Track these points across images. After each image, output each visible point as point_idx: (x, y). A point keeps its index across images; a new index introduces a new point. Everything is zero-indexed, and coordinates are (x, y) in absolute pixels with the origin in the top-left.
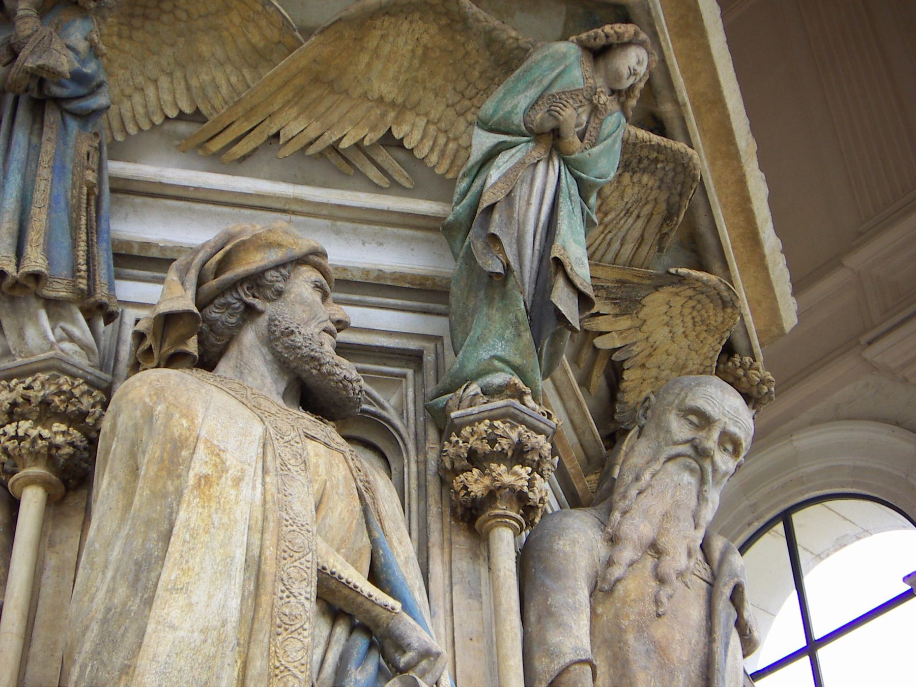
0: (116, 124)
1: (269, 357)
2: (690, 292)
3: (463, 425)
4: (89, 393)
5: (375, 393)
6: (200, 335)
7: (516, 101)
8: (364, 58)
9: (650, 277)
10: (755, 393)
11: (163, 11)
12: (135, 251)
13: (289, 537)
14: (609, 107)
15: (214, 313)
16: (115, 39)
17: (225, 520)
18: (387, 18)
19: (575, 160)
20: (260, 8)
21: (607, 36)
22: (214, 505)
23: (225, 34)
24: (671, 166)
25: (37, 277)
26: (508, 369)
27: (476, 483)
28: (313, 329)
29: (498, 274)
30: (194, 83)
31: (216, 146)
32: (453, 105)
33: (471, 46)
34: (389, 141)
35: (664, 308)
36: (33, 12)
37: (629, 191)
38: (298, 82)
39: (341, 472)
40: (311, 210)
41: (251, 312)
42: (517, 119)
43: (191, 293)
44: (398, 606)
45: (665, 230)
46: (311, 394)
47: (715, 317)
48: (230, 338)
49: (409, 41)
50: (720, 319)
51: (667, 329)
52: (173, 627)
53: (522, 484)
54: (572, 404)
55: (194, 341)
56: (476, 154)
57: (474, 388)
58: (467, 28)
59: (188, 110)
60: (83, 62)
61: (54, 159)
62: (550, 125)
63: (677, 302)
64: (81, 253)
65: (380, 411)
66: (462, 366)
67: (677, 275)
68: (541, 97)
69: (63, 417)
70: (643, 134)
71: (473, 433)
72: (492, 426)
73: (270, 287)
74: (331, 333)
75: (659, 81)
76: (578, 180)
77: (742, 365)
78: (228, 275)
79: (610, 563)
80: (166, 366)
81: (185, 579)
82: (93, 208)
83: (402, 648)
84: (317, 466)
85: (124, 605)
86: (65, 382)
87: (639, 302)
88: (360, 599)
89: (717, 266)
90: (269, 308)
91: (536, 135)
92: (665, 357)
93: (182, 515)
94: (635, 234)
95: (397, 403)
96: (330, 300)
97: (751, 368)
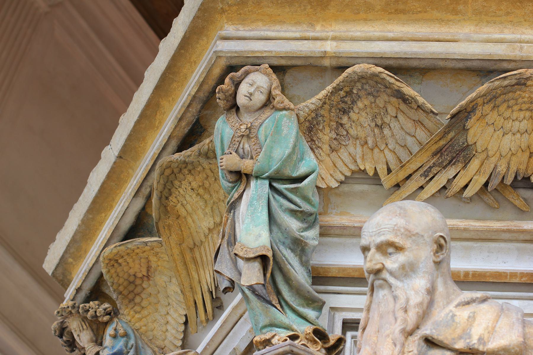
0: (172, 348)
2: (487, 108)
8: (190, 220)
9: (445, 133)
11: (141, 285)
16: (137, 316)
18: (170, 198)
19: (256, 173)
23: (160, 268)
35: (491, 129)
37: (362, 119)
38: (188, 257)
45: (414, 106)
49: (190, 194)
51: (509, 136)
60: (113, 347)
63: (493, 117)
67: (453, 116)
87: (468, 146)
94: (409, 125)
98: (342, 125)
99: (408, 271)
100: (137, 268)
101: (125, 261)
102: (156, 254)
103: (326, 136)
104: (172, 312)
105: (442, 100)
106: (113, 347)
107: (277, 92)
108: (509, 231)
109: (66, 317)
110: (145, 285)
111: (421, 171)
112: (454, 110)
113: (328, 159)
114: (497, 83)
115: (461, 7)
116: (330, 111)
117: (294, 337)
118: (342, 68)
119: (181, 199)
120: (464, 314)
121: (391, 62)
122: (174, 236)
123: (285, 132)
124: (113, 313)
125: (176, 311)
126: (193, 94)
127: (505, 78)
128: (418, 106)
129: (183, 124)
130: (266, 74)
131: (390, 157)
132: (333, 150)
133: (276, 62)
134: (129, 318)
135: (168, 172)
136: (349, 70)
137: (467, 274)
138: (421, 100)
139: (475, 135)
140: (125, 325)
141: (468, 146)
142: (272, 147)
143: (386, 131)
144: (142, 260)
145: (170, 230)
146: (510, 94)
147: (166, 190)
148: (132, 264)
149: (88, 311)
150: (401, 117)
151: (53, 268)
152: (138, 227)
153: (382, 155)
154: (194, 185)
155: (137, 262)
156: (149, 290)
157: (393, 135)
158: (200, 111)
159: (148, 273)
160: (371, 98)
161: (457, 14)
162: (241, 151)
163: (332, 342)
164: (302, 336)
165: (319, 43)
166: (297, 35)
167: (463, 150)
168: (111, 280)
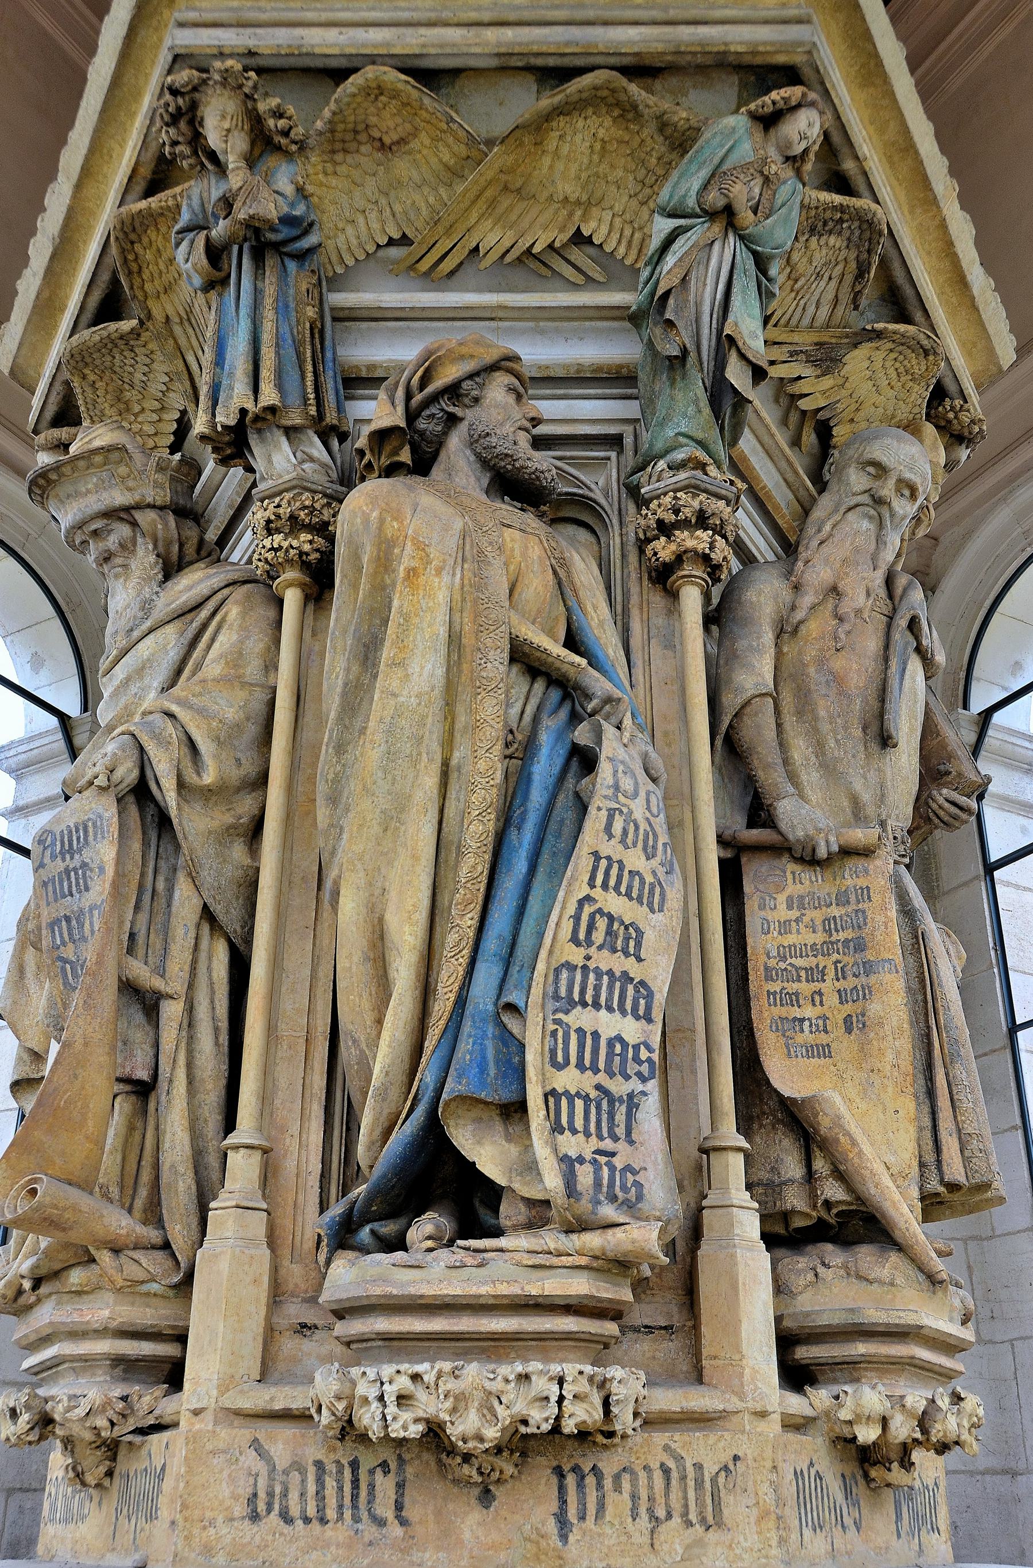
0: (334, 258)
1: (472, 458)
2: (890, 345)
3: (651, 500)
4: (329, 505)
5: (582, 477)
6: (410, 443)
7: (687, 184)
8: (547, 161)
10: (966, 434)
11: (360, 143)
12: (364, 374)
13: (485, 613)
14: (782, 175)
15: (422, 424)
17: (431, 604)
19: (749, 235)
20: (445, 127)
21: (774, 103)
22: (421, 592)
23: (418, 156)
24: (856, 224)
25: (272, 409)
26: (692, 443)
27: (664, 550)
28: (508, 429)
29: (676, 357)
30: (398, 208)
31: (425, 265)
32: (636, 195)
33: (645, 133)
34: (579, 239)
35: (867, 364)
36: (243, 164)
37: (817, 255)
38: (489, 193)
39: (536, 552)
40: (516, 314)
41: (452, 420)
42: (691, 202)
43: (400, 409)
44: (584, 662)
45: (858, 288)
46: (511, 485)
47: (918, 365)
48: (439, 444)
50: (924, 368)
51: (870, 383)
52: (395, 695)
53: (703, 547)
54: (783, 464)
55: (412, 452)
56: (655, 243)
57: (662, 464)
58: (639, 115)
59: (396, 236)
60: (292, 205)
61: (277, 300)
62: (721, 203)
64: (309, 383)
65: (587, 493)
66: (651, 445)
67: (873, 330)
68: (713, 175)
69: (309, 528)
70: (826, 197)
71: (659, 506)
72: (675, 498)
73: (467, 395)
74: (527, 430)
75: (836, 138)
76: (755, 254)
77: (952, 408)
78: (430, 389)
79: (793, 608)
80: (387, 476)
81: (402, 656)
82: (317, 341)
83: (589, 697)
84: (512, 550)
85: (358, 679)
86: (306, 498)
88: (550, 659)
89: (918, 316)
90: (469, 415)
91: (711, 215)
92: (873, 409)
93: (396, 603)
94: (830, 295)
95: (601, 482)
96: (524, 400)
97: (961, 410)
100: (389, 123)
102: (435, 139)
111: (792, 348)
122: (510, 160)
126: (732, 49)
129: (669, 58)
135: (605, 93)
148: (386, 114)
149: (281, 116)
154: (601, 133)
155: (399, 120)
156: (363, 160)
159: (393, 143)
167: (832, 360)
168: (344, 108)
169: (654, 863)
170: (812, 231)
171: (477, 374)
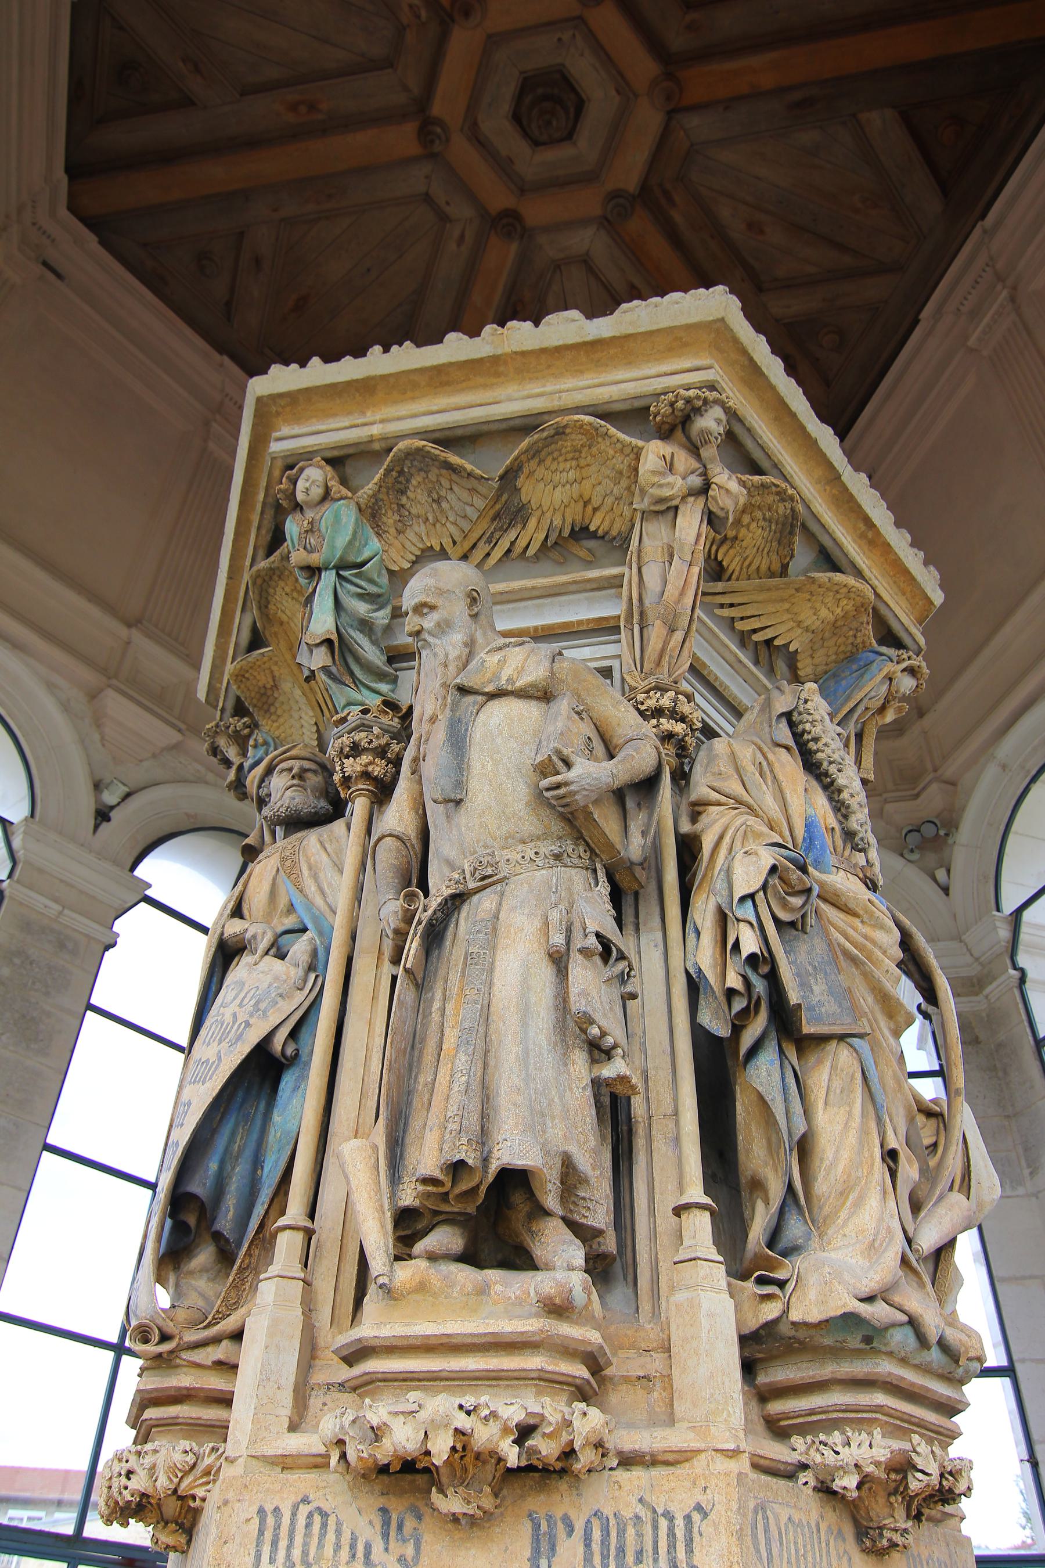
2: (533, 464)
8: (292, 625)
10: (680, 414)
16: (275, 725)
37: (419, 497)
50: (580, 436)
63: (540, 472)
87: (523, 505)
94: (465, 495)
98: (403, 506)
99: (444, 627)
101: (252, 674)
102: (276, 663)
103: (390, 519)
104: (303, 715)
105: (490, 463)
106: (254, 757)
107: (334, 485)
108: (575, 582)
109: (214, 737)
110: (276, 695)
112: (501, 471)
113: (396, 542)
114: (536, 436)
115: (502, 369)
116: (388, 493)
117: (365, 712)
118: (391, 450)
119: (279, 606)
120: (496, 658)
121: (437, 435)
123: (344, 520)
124: (254, 726)
125: (306, 714)
127: (543, 430)
128: (469, 474)
129: (263, 532)
130: (320, 467)
131: (452, 529)
132: (399, 532)
133: (329, 454)
134: (268, 728)
135: (259, 581)
136: (395, 450)
137: (536, 629)
138: (469, 467)
139: (527, 494)
140: (265, 735)
141: (523, 505)
142: (333, 537)
143: (444, 505)
144: (267, 671)
145: (277, 637)
146: (553, 446)
147: (263, 600)
148: (258, 677)
150: (455, 488)
151: (205, 695)
152: (256, 641)
153: (445, 529)
154: (287, 589)
155: (262, 673)
156: (281, 699)
157: (451, 508)
158: (275, 517)
159: (274, 681)
160: (422, 474)
161: (499, 377)
162: (308, 546)
163: (404, 711)
164: (374, 709)
165: (366, 428)
166: (347, 424)
167: (519, 510)
169: (223, 1044)
170: (403, 492)
171: (262, 781)
